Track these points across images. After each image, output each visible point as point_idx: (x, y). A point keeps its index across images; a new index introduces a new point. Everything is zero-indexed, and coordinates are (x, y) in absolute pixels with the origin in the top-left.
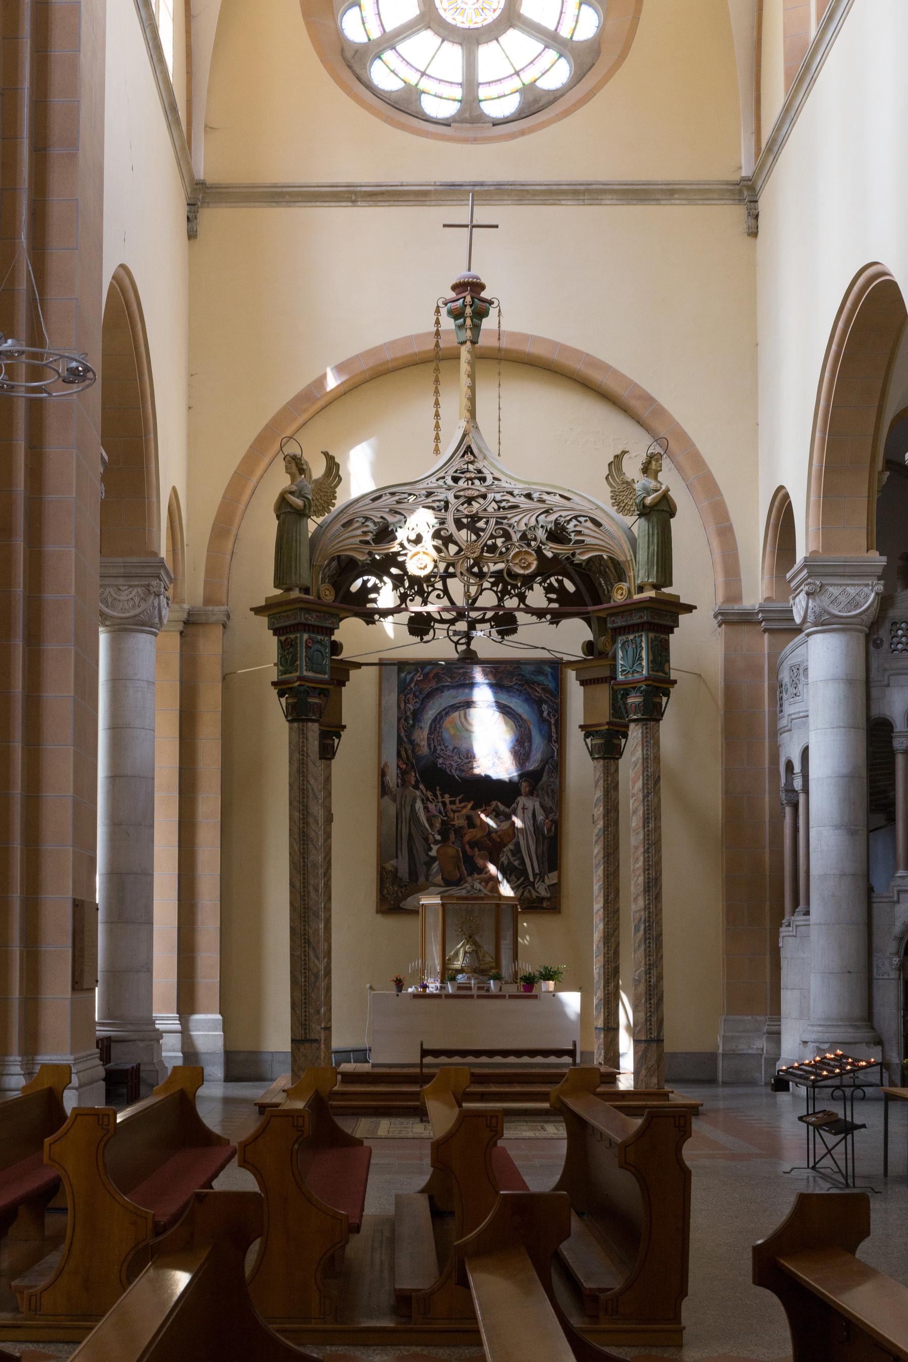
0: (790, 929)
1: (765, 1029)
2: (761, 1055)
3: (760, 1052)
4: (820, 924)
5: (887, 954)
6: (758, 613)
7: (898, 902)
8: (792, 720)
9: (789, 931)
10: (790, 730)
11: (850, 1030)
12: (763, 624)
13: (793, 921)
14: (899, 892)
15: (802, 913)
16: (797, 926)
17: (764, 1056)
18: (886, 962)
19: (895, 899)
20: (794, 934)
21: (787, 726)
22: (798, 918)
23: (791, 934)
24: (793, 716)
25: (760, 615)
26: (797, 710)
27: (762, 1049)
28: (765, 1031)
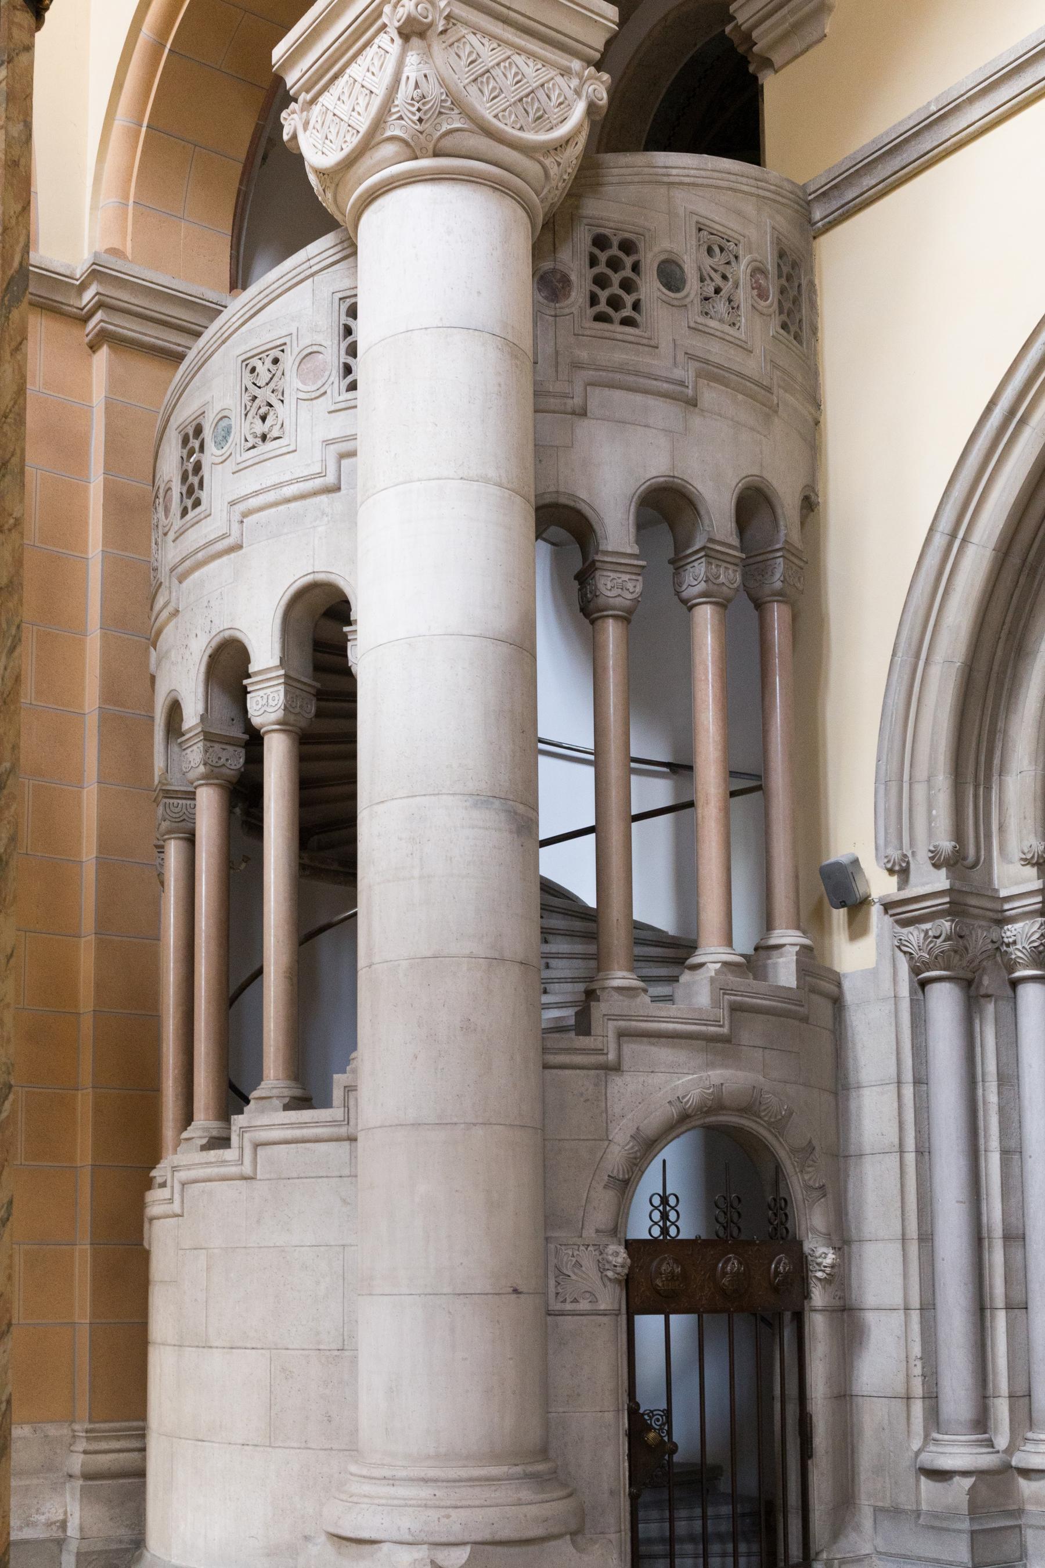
0: (229, 1154)
1: (76, 1463)
2: (60, 1543)
3: (57, 1534)
4: (416, 1125)
5: (589, 1233)
6: (83, 287)
7: (616, 1068)
8: (245, 515)
9: (223, 1163)
10: (237, 547)
11: (525, 1494)
12: (99, 315)
13: (243, 1130)
14: (622, 1035)
15: (278, 1103)
16: (257, 1146)
17: (73, 1546)
18: (588, 1260)
19: (612, 1056)
20: (247, 1169)
21: (224, 537)
22: (265, 1120)
23: (233, 1170)
24: (254, 502)
25: (88, 295)
26: (276, 480)
27: (63, 1525)
28: (77, 1469)
